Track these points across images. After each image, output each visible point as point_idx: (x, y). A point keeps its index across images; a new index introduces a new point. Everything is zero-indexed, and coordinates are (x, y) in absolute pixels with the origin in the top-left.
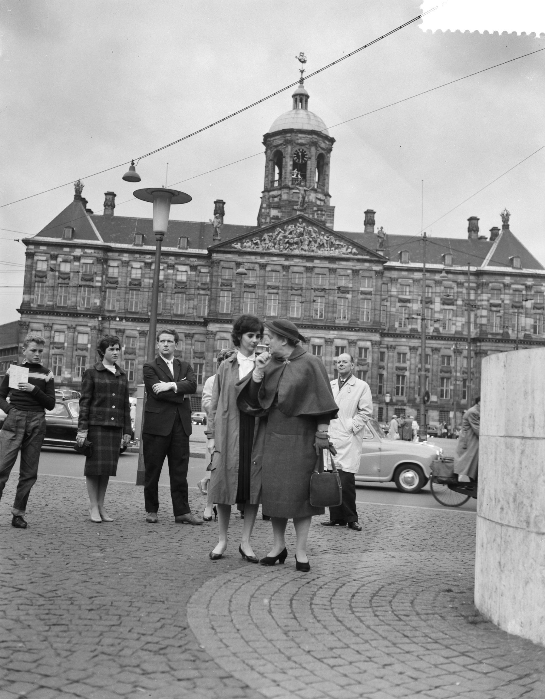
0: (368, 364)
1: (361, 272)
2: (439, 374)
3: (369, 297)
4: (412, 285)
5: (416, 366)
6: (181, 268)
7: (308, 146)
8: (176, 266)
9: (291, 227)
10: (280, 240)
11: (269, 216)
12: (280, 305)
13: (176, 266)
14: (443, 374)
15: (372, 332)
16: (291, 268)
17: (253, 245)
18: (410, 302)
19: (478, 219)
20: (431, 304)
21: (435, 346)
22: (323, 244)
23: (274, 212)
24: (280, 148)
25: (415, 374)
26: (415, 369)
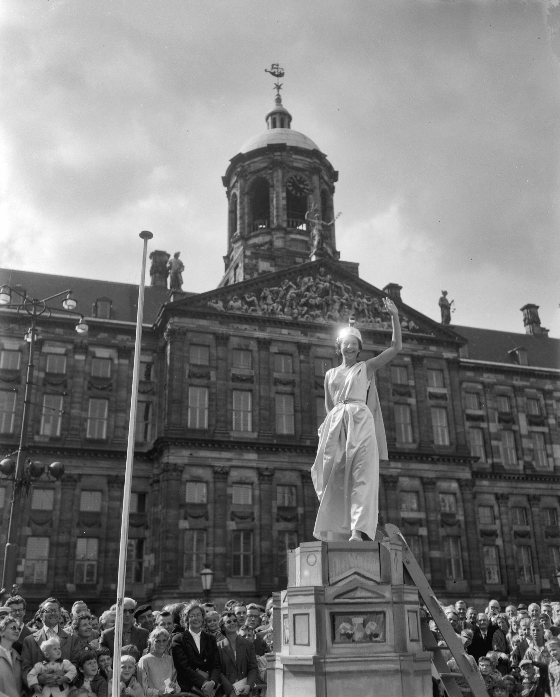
0: (458, 523)
1: (425, 362)
2: (545, 540)
3: (443, 403)
4: (482, 393)
5: (511, 529)
6: (102, 353)
7: (308, 173)
8: (91, 349)
9: (308, 280)
10: (292, 299)
11: (257, 270)
12: (299, 415)
13: (91, 349)
14: (550, 540)
15: (458, 464)
16: (313, 349)
17: (245, 307)
18: (483, 421)
19: (538, 307)
20: (514, 423)
21: (532, 492)
22: (363, 311)
23: (264, 266)
24: (263, 174)
25: (510, 542)
26: (510, 534)
